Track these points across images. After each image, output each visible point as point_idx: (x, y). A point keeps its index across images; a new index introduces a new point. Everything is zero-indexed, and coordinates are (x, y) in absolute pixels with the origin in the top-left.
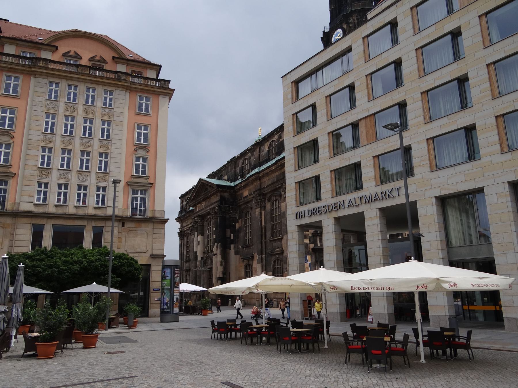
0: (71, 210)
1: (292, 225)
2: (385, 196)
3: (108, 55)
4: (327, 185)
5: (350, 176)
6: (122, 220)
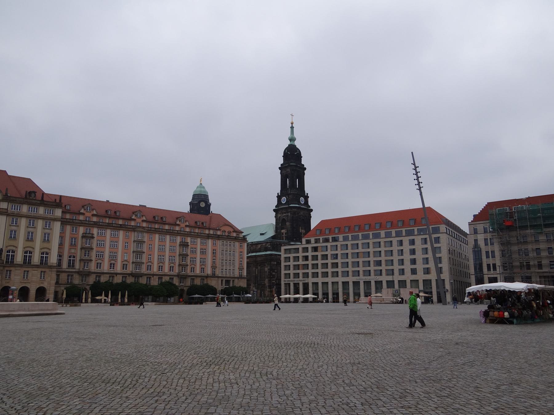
0: (228, 276)
1: (283, 283)
2: (304, 280)
3: (232, 230)
4: (292, 276)
5: (297, 275)
6: (238, 278)
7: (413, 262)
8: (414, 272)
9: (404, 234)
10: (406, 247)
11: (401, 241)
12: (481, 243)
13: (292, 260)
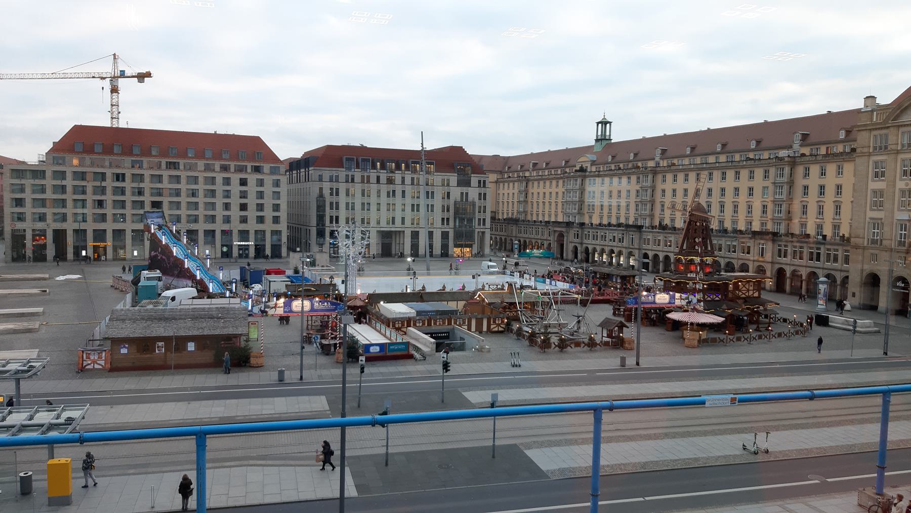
7: (243, 207)
8: (244, 220)
9: (232, 169)
10: (235, 188)
11: (229, 179)
12: (326, 192)
13: (28, 190)
